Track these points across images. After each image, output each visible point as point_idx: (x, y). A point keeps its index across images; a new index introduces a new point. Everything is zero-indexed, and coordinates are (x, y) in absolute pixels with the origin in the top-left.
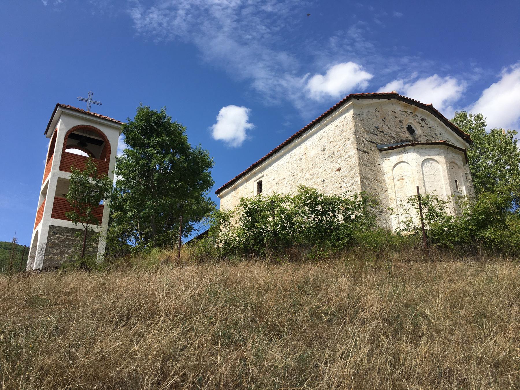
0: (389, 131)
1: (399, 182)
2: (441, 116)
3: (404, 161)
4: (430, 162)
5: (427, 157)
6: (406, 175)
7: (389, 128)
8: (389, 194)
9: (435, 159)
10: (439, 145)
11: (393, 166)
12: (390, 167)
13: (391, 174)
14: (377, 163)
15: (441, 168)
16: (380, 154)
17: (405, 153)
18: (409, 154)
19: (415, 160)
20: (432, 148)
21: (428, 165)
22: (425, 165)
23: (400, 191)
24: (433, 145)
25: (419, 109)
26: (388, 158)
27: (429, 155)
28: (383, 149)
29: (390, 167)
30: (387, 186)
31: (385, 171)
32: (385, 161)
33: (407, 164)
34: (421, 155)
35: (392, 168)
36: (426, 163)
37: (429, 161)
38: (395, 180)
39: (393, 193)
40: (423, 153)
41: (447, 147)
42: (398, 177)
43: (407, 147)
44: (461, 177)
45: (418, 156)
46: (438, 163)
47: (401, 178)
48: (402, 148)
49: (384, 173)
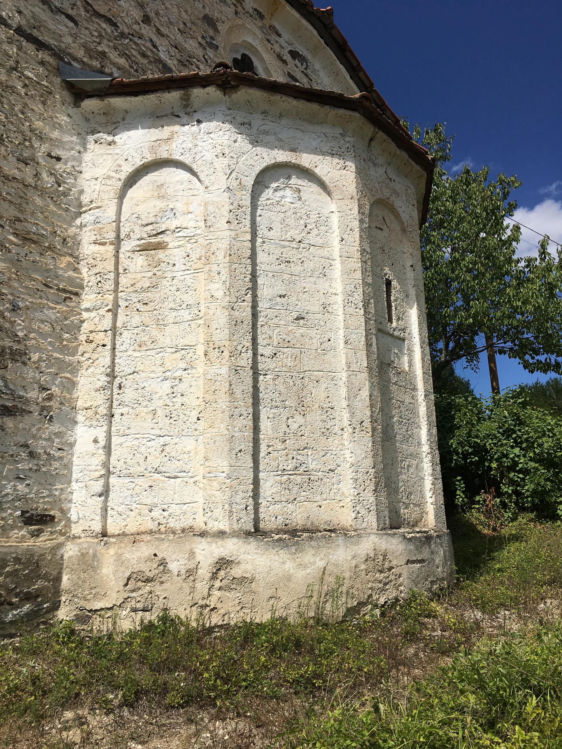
0: (146, 30)
1: (140, 260)
2: (355, 64)
3: (177, 156)
4: (294, 181)
5: (282, 156)
6: (179, 229)
7: (147, 20)
8: (85, 315)
9: (317, 171)
10: (341, 111)
11: (123, 176)
12: (109, 177)
13: (111, 212)
14: (42, 149)
15: (335, 220)
16: (72, 111)
17: (185, 119)
18: (203, 125)
19: (226, 161)
20: (312, 120)
21: (279, 194)
22: (268, 193)
23: (138, 306)
24: (315, 106)
25: (288, 8)
26: (110, 138)
27: (293, 150)
28: (88, 88)
29: (109, 177)
30: (84, 271)
31: (85, 199)
32: (91, 146)
33: (185, 175)
34: (255, 142)
35: (120, 184)
36: (274, 185)
37: (289, 178)
38: (126, 246)
39: (102, 312)
40: (266, 133)
41: (369, 129)
42: (139, 232)
43: (197, 92)
44: (409, 269)
45: (243, 143)
46: (329, 194)
47: (153, 240)
48: (174, 96)
49: (80, 206)
